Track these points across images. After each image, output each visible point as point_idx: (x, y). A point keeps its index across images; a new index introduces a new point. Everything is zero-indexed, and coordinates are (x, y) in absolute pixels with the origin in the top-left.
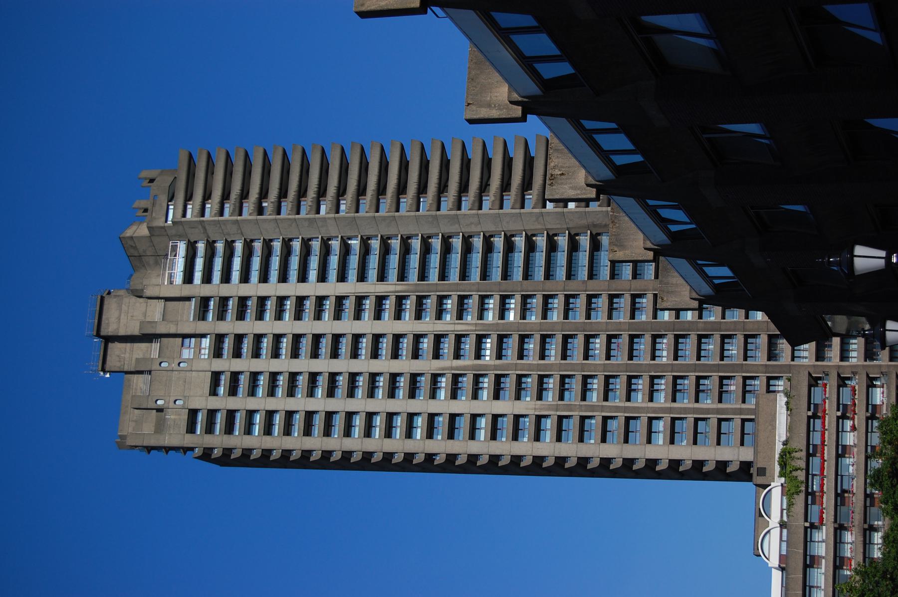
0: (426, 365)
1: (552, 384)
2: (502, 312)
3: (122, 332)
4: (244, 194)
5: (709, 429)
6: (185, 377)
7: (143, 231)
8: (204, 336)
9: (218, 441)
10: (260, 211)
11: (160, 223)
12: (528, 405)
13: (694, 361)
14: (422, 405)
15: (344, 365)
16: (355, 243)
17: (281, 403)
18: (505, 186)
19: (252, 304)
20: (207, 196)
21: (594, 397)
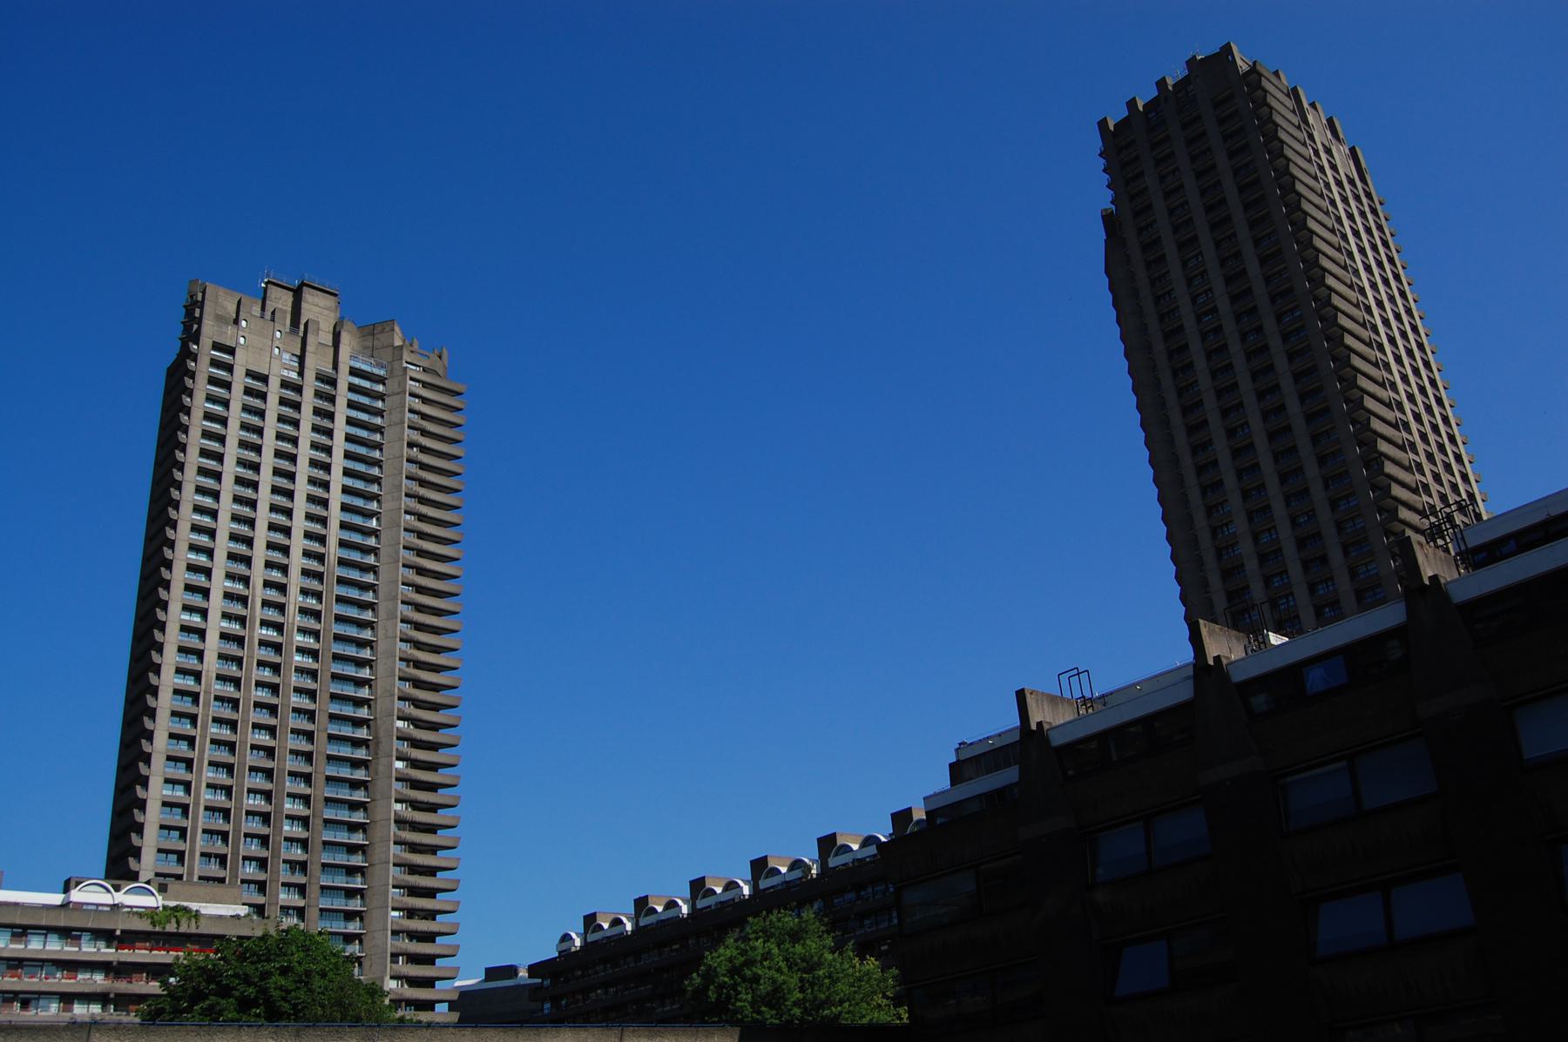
0: (258, 573)
1: (229, 690)
2: (301, 650)
3: (304, 305)
4: (424, 433)
5: (174, 842)
6: (262, 348)
7: (398, 342)
8: (301, 374)
9: (203, 369)
10: (411, 445)
11: (406, 356)
12: (211, 665)
13: (244, 830)
14: (220, 564)
15: (265, 497)
16: (374, 523)
17: (234, 433)
18: (418, 665)
20: (425, 400)
21: (214, 730)
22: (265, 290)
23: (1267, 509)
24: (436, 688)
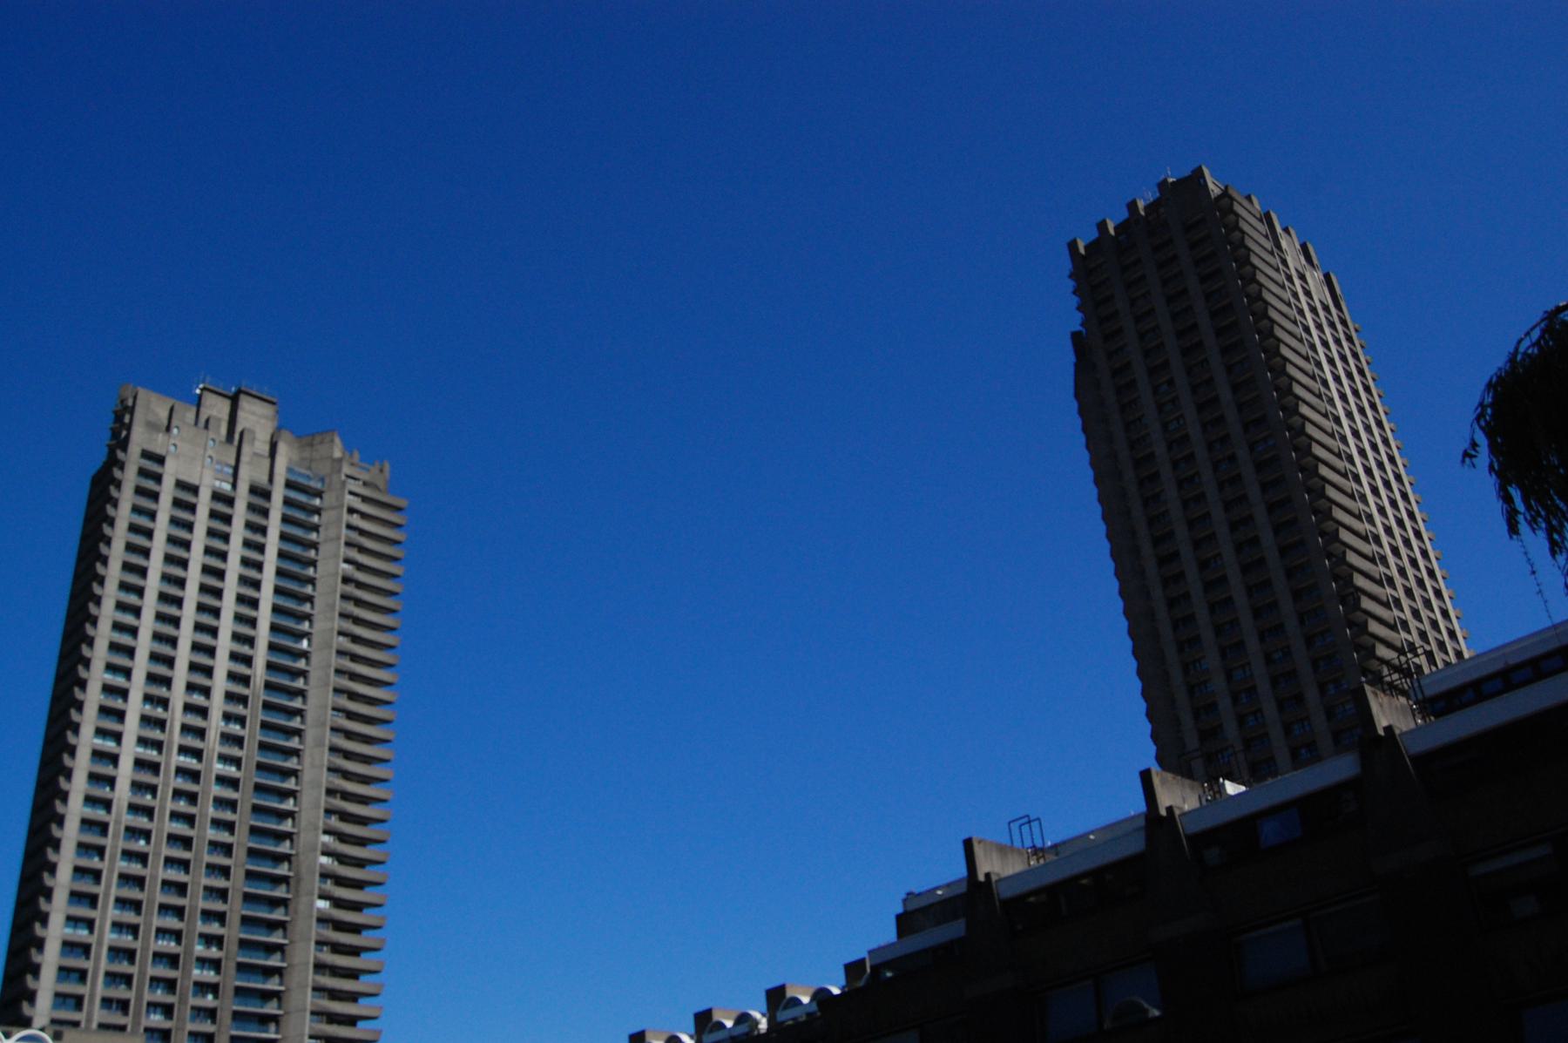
3: (241, 414)
6: (192, 459)
7: (337, 454)
8: (234, 486)
11: (346, 469)
19: (258, 538)
20: (364, 516)
22: (200, 397)
23: (1240, 645)
24: (363, 821)
